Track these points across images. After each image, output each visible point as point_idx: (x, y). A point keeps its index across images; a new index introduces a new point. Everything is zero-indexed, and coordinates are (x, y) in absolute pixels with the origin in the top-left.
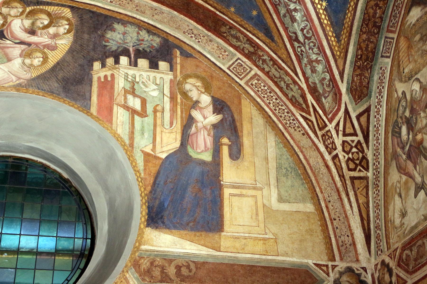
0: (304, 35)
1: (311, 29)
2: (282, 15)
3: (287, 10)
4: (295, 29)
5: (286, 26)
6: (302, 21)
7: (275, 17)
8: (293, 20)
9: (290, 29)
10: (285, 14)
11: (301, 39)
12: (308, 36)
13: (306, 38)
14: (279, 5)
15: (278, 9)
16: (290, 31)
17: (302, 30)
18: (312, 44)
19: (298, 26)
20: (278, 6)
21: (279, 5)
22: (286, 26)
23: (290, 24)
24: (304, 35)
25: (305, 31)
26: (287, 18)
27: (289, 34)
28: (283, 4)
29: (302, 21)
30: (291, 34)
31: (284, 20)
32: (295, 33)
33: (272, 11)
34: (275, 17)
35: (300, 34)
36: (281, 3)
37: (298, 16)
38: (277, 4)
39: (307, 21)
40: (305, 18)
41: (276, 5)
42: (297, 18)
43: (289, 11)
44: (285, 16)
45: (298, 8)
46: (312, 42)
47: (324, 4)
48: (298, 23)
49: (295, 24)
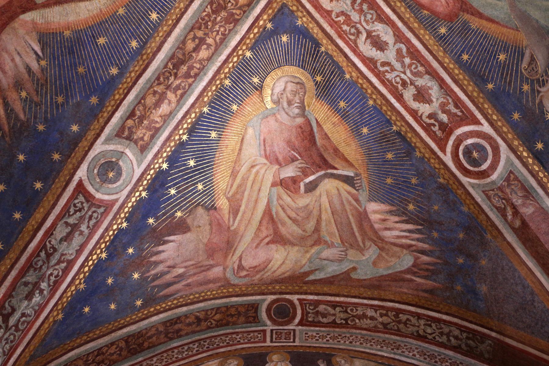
0: (19, 321)
1: (28, 323)
2: (24, 280)
3: (36, 283)
4: (19, 306)
5: (14, 293)
6: (32, 307)
7: (14, 273)
8: (29, 297)
9: (14, 301)
10: (29, 283)
11: (12, 321)
12: (20, 326)
13: (16, 326)
14: (35, 269)
15: (28, 271)
16: (10, 301)
17: (23, 315)
18: (12, 337)
19: (26, 307)
20: (32, 269)
21: (35, 269)
22: (14, 293)
23: (21, 297)
24: (19, 321)
25: (24, 318)
26: (26, 288)
27: (5, 303)
28: (41, 273)
29: (32, 307)
30: (7, 305)
31: (19, 287)
32: (14, 310)
33: (19, 266)
34: (14, 273)
35: (17, 315)
36: (40, 271)
37: (37, 299)
38: (33, 267)
39: (35, 312)
40: (37, 308)
41: (31, 266)
42: (34, 300)
43: (36, 285)
44: (26, 284)
45: (45, 292)
46: (15, 336)
47: (60, 317)
48: (28, 305)
49: (26, 303)
